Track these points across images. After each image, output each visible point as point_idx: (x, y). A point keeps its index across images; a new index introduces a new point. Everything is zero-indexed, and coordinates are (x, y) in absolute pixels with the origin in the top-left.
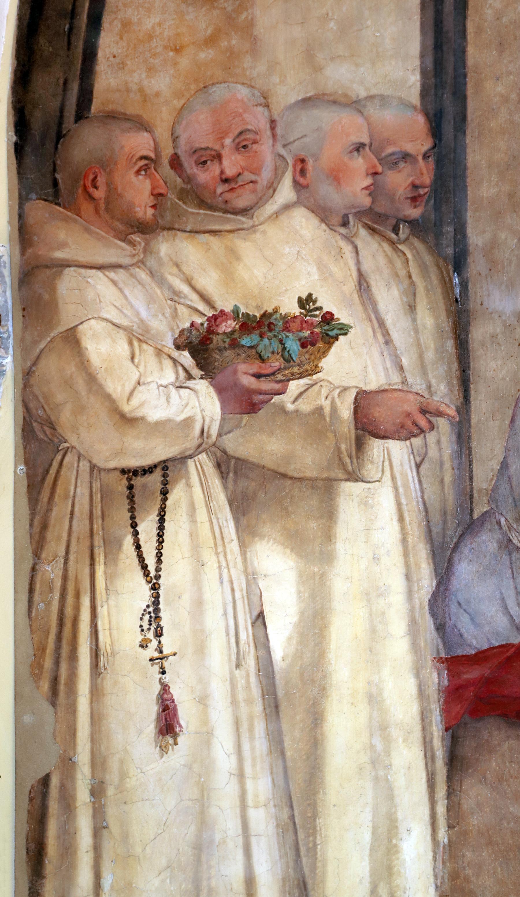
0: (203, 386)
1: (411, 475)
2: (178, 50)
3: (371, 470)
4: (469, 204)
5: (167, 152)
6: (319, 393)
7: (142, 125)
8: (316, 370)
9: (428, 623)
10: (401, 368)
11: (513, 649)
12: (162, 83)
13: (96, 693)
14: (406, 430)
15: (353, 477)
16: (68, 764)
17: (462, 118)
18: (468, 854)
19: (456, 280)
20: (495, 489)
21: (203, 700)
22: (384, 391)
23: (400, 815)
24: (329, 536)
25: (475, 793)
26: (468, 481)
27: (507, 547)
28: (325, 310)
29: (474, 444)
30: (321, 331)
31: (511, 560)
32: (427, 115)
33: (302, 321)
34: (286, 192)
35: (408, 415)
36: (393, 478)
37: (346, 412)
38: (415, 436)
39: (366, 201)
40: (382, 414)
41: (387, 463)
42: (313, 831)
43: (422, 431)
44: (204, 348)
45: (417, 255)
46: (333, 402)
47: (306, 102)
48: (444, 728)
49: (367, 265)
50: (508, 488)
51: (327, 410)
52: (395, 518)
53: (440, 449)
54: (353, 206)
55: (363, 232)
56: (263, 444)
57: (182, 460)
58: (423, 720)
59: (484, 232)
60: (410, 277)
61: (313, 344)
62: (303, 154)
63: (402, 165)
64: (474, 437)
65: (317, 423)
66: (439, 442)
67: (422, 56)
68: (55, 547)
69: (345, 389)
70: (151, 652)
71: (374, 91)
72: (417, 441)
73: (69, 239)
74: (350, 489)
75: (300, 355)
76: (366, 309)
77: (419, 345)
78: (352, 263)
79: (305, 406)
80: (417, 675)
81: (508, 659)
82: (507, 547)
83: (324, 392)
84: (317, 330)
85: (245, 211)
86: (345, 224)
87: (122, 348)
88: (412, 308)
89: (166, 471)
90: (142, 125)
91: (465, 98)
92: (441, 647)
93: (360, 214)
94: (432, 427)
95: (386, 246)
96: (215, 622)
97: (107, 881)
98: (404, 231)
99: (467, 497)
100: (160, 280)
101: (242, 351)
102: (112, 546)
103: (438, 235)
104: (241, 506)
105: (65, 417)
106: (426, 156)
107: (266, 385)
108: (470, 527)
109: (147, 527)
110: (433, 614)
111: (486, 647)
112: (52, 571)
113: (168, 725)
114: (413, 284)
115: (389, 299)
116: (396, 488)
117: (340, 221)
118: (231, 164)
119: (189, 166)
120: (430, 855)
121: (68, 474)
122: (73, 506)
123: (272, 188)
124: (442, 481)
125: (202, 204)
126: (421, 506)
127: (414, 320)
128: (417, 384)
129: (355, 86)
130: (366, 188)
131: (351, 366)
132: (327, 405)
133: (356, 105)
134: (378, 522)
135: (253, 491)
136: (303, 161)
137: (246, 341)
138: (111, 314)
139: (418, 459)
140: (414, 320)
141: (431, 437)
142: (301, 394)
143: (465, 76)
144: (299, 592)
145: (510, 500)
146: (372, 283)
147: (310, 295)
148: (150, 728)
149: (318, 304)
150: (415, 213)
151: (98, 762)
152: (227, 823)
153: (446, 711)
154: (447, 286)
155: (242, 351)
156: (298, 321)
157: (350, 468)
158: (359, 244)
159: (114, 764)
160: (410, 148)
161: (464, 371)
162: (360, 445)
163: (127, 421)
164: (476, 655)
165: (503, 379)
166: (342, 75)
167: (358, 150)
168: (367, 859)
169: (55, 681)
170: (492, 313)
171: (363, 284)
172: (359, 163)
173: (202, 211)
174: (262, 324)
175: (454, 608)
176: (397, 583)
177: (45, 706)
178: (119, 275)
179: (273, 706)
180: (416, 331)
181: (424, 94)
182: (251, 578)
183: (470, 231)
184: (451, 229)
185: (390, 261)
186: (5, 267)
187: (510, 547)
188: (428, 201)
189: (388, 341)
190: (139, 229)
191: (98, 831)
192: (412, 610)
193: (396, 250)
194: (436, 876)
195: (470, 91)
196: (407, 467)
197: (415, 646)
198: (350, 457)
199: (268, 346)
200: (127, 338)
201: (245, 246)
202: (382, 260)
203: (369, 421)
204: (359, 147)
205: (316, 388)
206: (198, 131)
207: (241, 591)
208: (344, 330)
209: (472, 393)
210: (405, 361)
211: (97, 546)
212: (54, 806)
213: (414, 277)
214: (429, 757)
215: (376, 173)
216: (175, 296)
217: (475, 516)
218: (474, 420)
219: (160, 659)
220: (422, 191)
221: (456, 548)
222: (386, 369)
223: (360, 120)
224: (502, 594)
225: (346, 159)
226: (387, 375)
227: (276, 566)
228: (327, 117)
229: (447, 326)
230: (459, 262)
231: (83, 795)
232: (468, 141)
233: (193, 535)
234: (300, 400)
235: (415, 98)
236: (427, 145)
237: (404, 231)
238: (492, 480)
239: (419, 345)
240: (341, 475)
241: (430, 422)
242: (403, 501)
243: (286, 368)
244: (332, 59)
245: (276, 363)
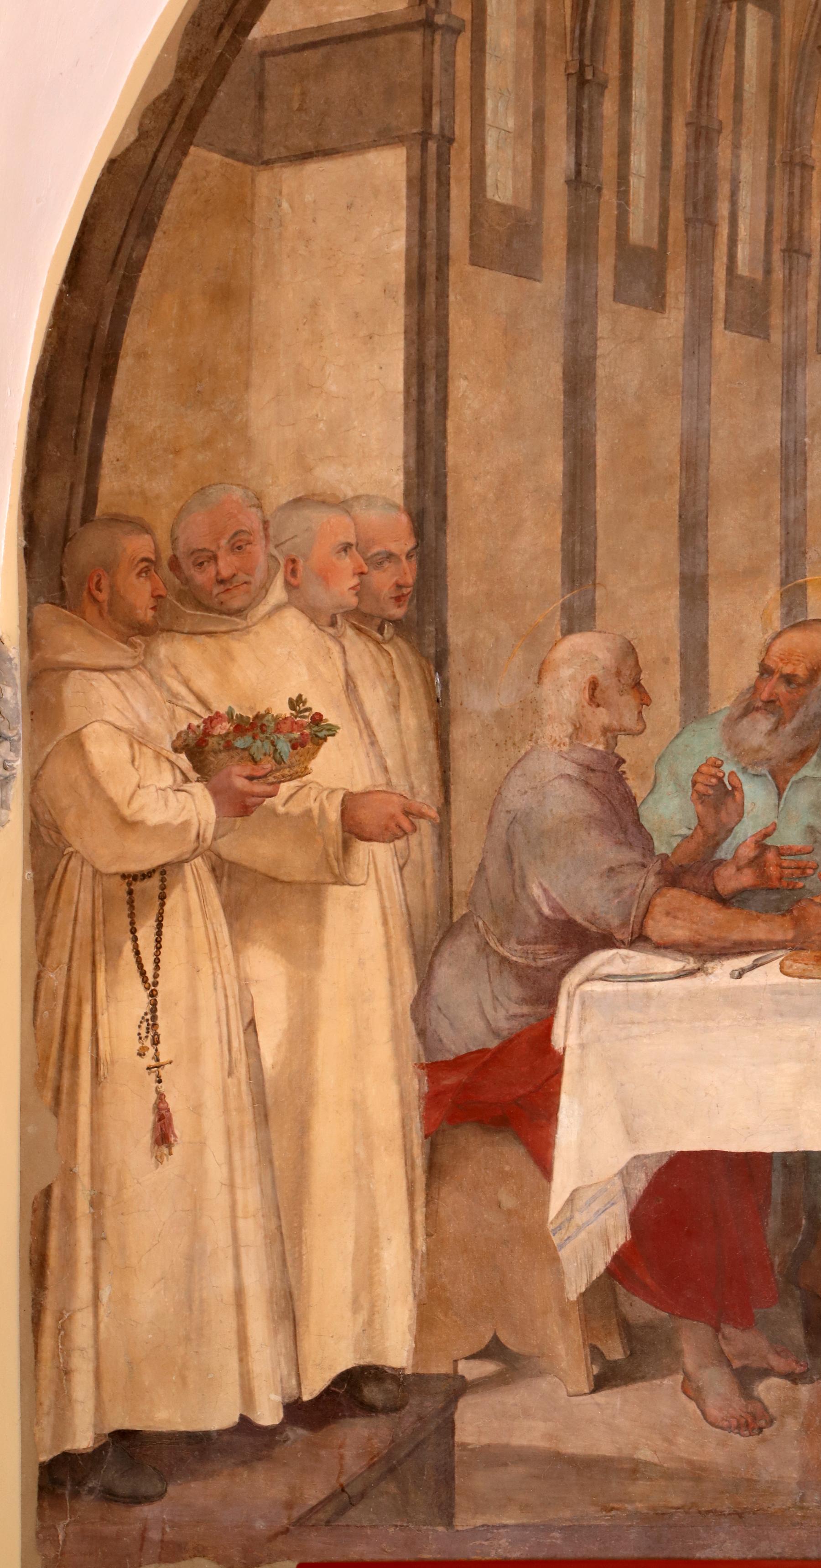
0: (198, 789)
1: (395, 878)
2: (177, 452)
3: (356, 873)
4: (449, 603)
5: (166, 554)
6: (308, 795)
7: (144, 528)
8: (306, 772)
9: (410, 1028)
10: (386, 769)
11: (489, 1054)
12: (161, 486)
13: (96, 1102)
14: (391, 832)
15: (340, 880)
16: (69, 1174)
17: (443, 518)
18: (445, 1262)
19: (438, 680)
20: (473, 892)
21: (197, 1110)
22: (370, 792)
23: (381, 1224)
24: (317, 941)
25: (452, 1199)
26: (448, 883)
27: (484, 950)
28: (314, 711)
29: (454, 846)
30: (313, 732)
31: (488, 963)
32: (410, 514)
33: (294, 723)
34: (277, 593)
35: (393, 817)
36: (378, 881)
37: (334, 815)
38: (398, 838)
39: (352, 601)
40: (366, 815)
41: (372, 866)
42: (299, 1241)
43: (405, 833)
44: (199, 751)
45: (401, 655)
46: (321, 804)
47: (298, 502)
48: (423, 1135)
49: (354, 666)
50: (486, 890)
51: (316, 812)
52: (380, 921)
53: (422, 851)
54: (341, 607)
55: (350, 632)
56: (256, 848)
57: (179, 863)
58: (404, 1127)
59: (463, 631)
60: (394, 677)
61: (303, 746)
62: (294, 554)
63: (386, 564)
64: (454, 838)
65: (305, 825)
66: (421, 844)
67: (406, 456)
68: (59, 954)
69: (333, 791)
70: (149, 1060)
71: (361, 491)
72: (400, 843)
73: (74, 643)
74: (337, 893)
75: (291, 756)
76: (353, 710)
77: (403, 746)
78: (339, 663)
79: (295, 808)
80: (399, 1081)
81: (485, 1064)
82: (484, 950)
83: (313, 794)
84: (307, 731)
85: (239, 612)
86: (333, 624)
87: (124, 751)
88: (396, 708)
89: (164, 875)
90: (144, 528)
91: (445, 498)
92: (422, 1052)
93: (347, 614)
94: (415, 829)
95: (372, 646)
96: (209, 1029)
97: (105, 1293)
98: (389, 631)
99: (447, 900)
100: (160, 683)
101: (234, 752)
102: (113, 953)
103: (421, 635)
104: (235, 911)
105: (70, 822)
106: (409, 556)
107: (259, 788)
108: (450, 930)
109: (146, 933)
110: (415, 1019)
111: (464, 1052)
112: (55, 978)
113: (163, 1136)
114: (397, 684)
115: (375, 699)
116: (380, 892)
117: (327, 620)
118: (226, 565)
119: (186, 565)
120: (409, 1264)
121: (72, 879)
122: (76, 911)
123: (265, 588)
124: (424, 884)
125: (200, 605)
126: (404, 910)
127: (398, 720)
128: (402, 787)
129: (342, 486)
130: (353, 588)
131: (339, 768)
132: (315, 806)
133: (343, 505)
136: (294, 561)
137: (240, 743)
138: (113, 716)
139: (402, 862)
140: (398, 720)
141: (414, 839)
142: (291, 796)
143: (445, 475)
144: (289, 998)
145: (488, 902)
146: (359, 683)
147: (300, 696)
148: (147, 1139)
149: (308, 705)
150: (398, 612)
151: (97, 1174)
152: (218, 1234)
153: (426, 1118)
154: (429, 685)
155: (234, 752)
156: (289, 722)
157: (337, 871)
158: (346, 643)
159: (112, 1174)
160: (394, 547)
161: (445, 772)
162: (346, 847)
163: (129, 825)
164: (454, 1060)
165: (481, 780)
166: (330, 476)
167: (345, 550)
168: (350, 1269)
169: (58, 1090)
170: (471, 713)
171: (350, 684)
172: (347, 563)
173: (199, 613)
174: (252, 726)
175: (434, 1013)
176: (380, 986)
177: (49, 1116)
178: (121, 678)
179: (263, 1115)
180: (400, 731)
181: (407, 494)
182: (244, 984)
183: (450, 630)
184: (432, 628)
185: (376, 661)
186: (16, 669)
187: (488, 950)
188: (411, 601)
189: (374, 743)
190: (139, 631)
191: (97, 1243)
192: (395, 1015)
193: (381, 650)
194: (414, 1285)
195: (450, 491)
196: (391, 869)
197: (397, 1053)
198: (337, 860)
199: (260, 747)
201: (238, 647)
202: (368, 661)
203: (356, 823)
204: (346, 547)
205: (305, 790)
206: (196, 533)
207: (234, 997)
208: (332, 731)
209: (453, 793)
210: (389, 763)
211: (97, 953)
212: (55, 1216)
213: (398, 676)
214: (409, 1164)
215: (362, 573)
216: (174, 698)
217: (455, 919)
218: (454, 821)
219: (157, 1067)
220: (405, 591)
221: (435, 953)
222: (371, 770)
223: (347, 520)
224: (479, 998)
225: (334, 559)
226: (372, 776)
227: (267, 970)
228: (317, 517)
229: (429, 726)
230: (440, 662)
231: (83, 1206)
232: (448, 540)
233: (189, 940)
234: (290, 803)
235: (398, 498)
236: (410, 544)
237: (389, 631)
238: (470, 882)
239: (403, 746)
240: (329, 879)
241: (412, 824)
242: (387, 904)
243: (277, 770)
244: (321, 460)
245: (268, 765)
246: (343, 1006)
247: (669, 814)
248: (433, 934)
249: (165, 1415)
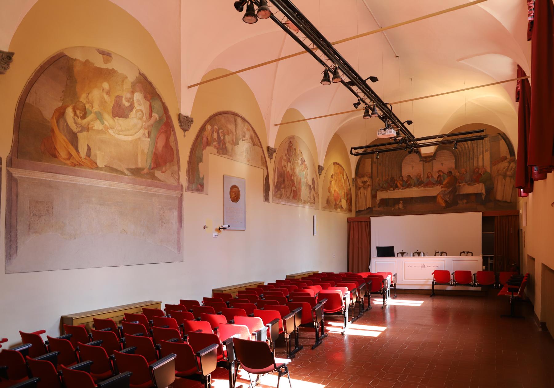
44: (363, 182)
101: (364, 182)
131: (368, 183)
134: (369, 189)
135: (365, 188)
200: (359, 182)
203: (369, 185)
246: (368, 193)
247: (381, 185)
248: (372, 190)
249: (361, 209)
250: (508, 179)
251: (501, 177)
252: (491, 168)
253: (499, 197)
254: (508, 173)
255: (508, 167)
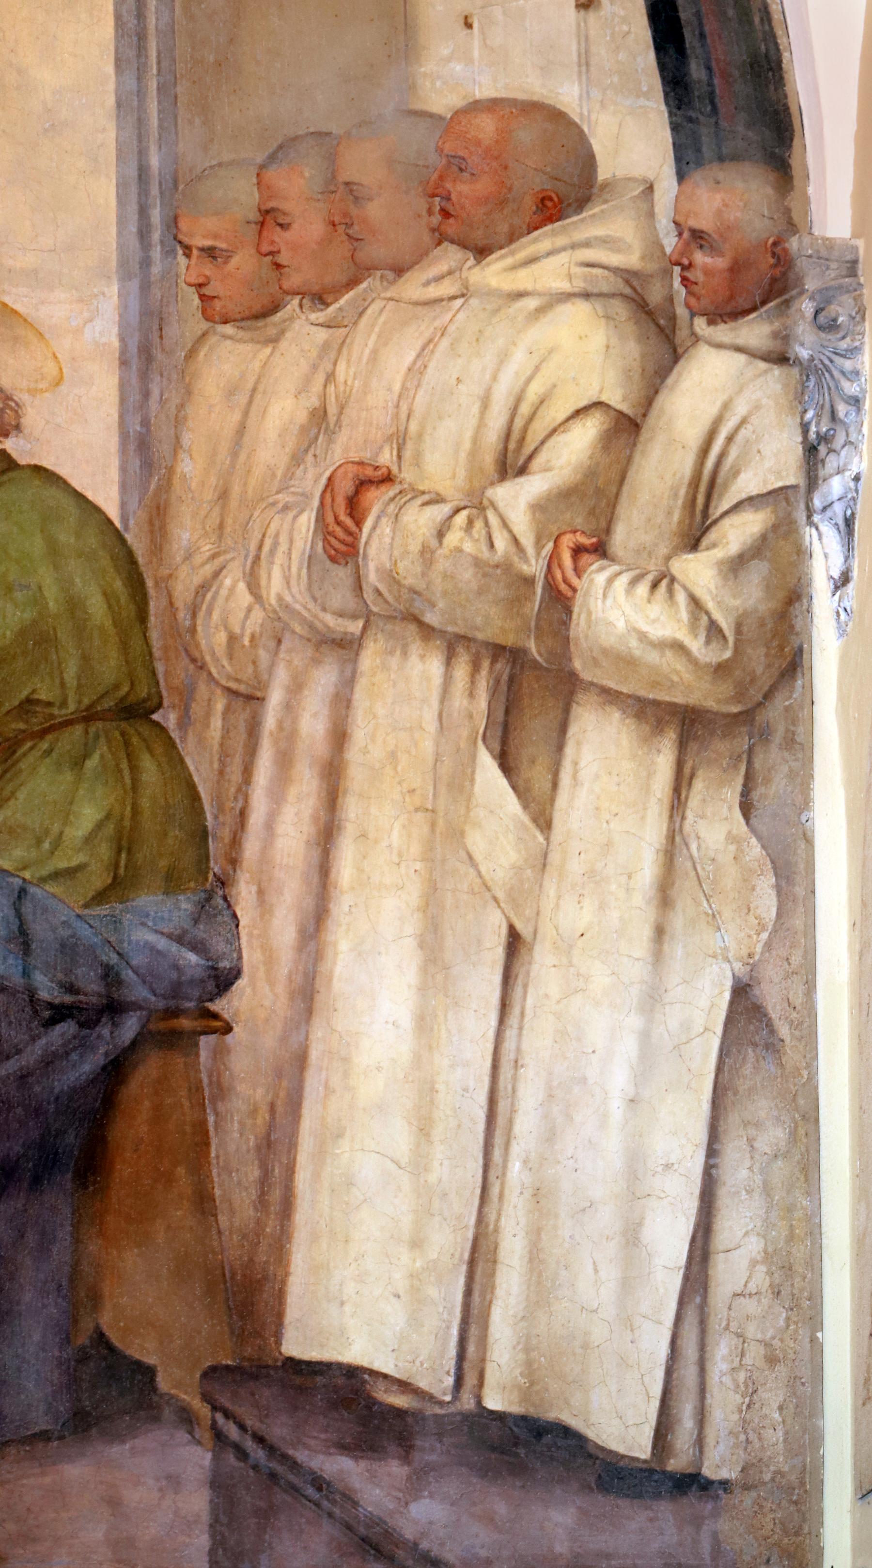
250: (608, 768)
251: (412, 703)
252: (149, 359)
253: (362, 1298)
254: (618, 612)
255: (627, 429)
